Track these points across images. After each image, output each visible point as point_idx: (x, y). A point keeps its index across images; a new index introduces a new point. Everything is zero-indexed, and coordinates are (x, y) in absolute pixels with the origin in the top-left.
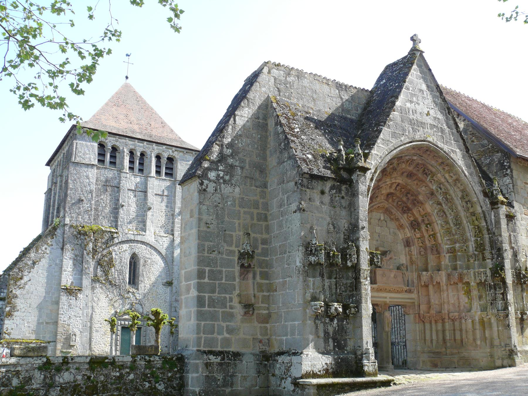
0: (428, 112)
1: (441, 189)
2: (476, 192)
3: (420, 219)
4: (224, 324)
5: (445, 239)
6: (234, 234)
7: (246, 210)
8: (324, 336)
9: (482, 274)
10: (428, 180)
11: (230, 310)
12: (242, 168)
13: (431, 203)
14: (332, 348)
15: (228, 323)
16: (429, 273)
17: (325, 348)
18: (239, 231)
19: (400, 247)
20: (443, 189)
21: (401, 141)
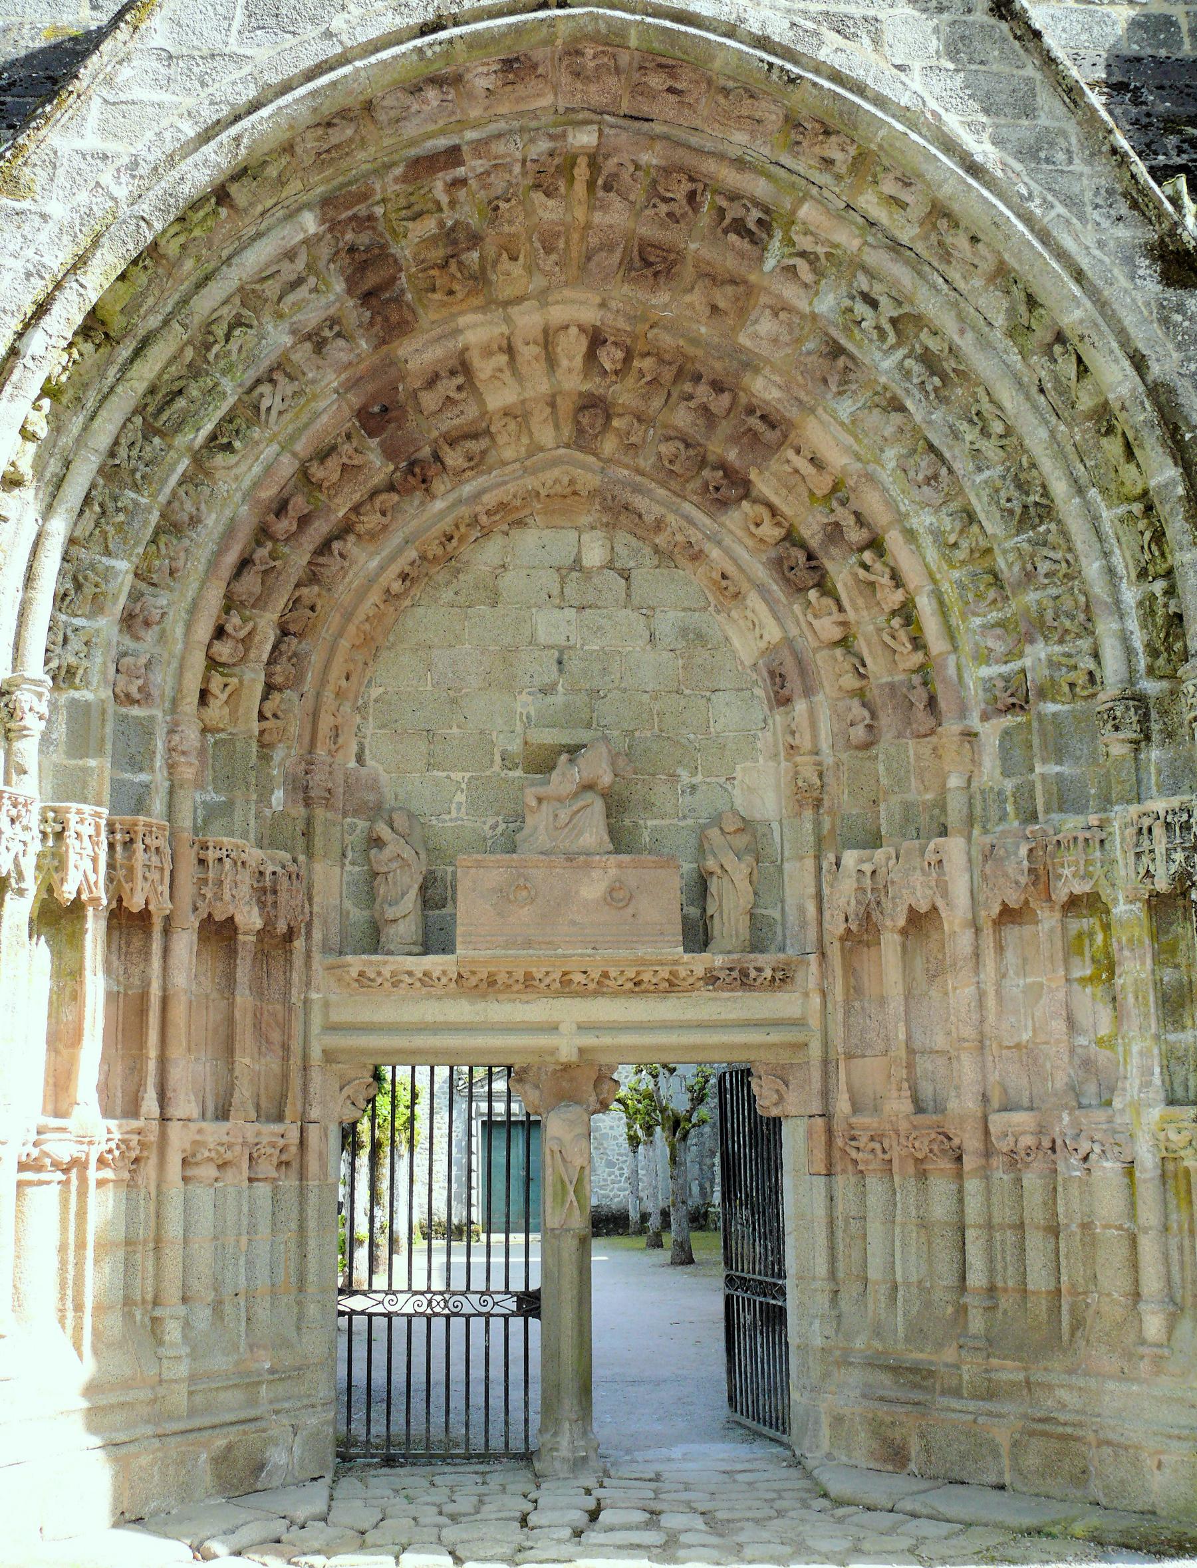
1: (874, 304)
2: (1084, 263)
3: (811, 529)
5: (978, 621)
9: (1158, 831)
10: (770, 263)
13: (846, 408)
16: (879, 854)
20: (884, 301)
21: (328, 35)
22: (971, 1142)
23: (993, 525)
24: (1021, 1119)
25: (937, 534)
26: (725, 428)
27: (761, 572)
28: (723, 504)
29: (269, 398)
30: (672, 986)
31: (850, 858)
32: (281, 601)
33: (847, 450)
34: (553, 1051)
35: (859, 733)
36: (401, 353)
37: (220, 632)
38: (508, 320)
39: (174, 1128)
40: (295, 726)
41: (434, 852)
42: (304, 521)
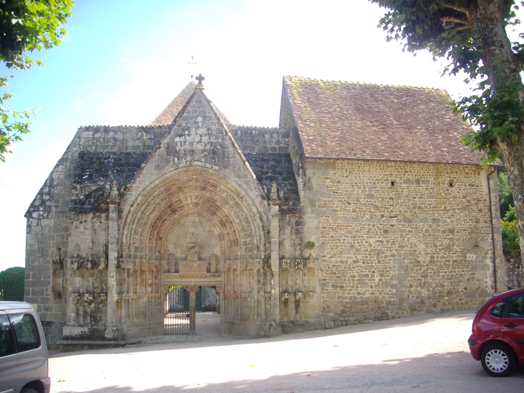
0: (201, 139)
1: (230, 196)
2: (252, 197)
4: (42, 305)
5: (242, 234)
6: (49, 250)
7: (58, 233)
8: (84, 314)
10: (218, 190)
11: (47, 297)
12: (56, 207)
13: (228, 206)
14: (89, 321)
15: (45, 304)
16: (231, 261)
17: (84, 321)
18: (53, 247)
19: (214, 241)
22: (239, 296)
23: (243, 223)
24: (244, 294)
25: (238, 222)
26: (213, 207)
27: (218, 223)
28: (214, 215)
29: (157, 207)
30: (205, 277)
31: (227, 261)
32: (158, 230)
33: (228, 212)
34: (191, 285)
35: (229, 245)
36: (172, 199)
37: (150, 235)
38: (186, 195)
39: (147, 295)
40: (159, 244)
41: (176, 259)
42: (160, 220)
